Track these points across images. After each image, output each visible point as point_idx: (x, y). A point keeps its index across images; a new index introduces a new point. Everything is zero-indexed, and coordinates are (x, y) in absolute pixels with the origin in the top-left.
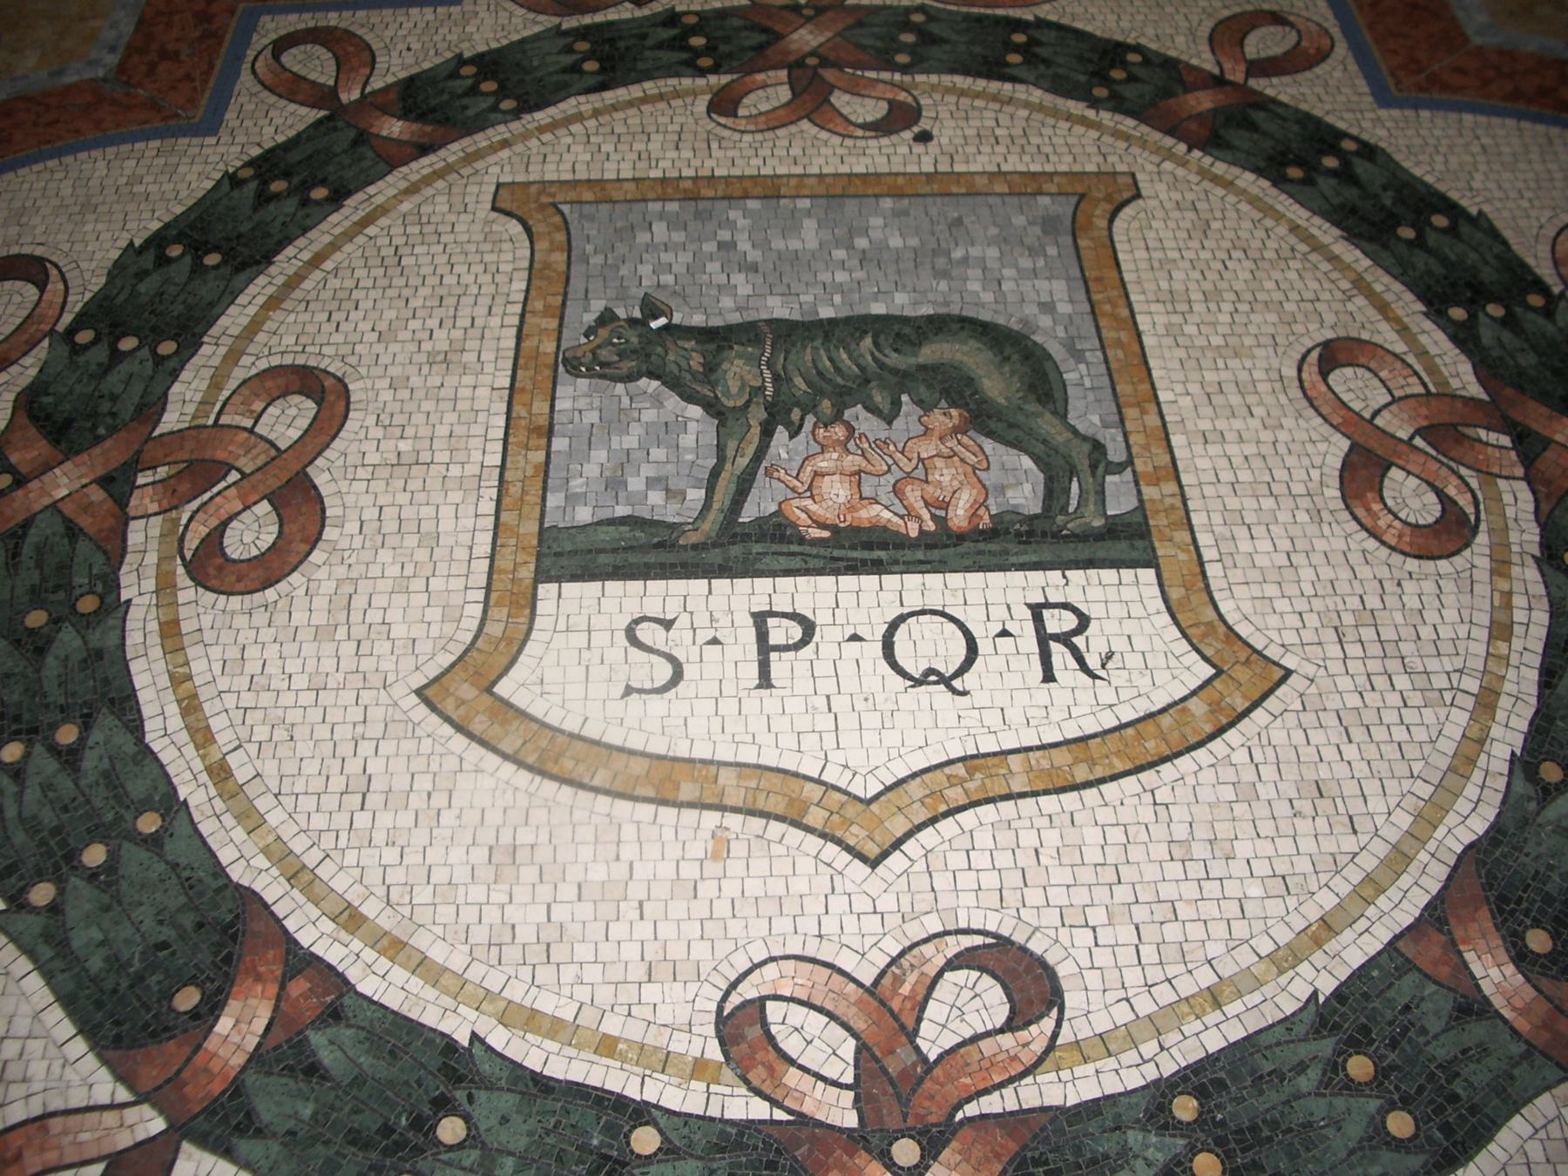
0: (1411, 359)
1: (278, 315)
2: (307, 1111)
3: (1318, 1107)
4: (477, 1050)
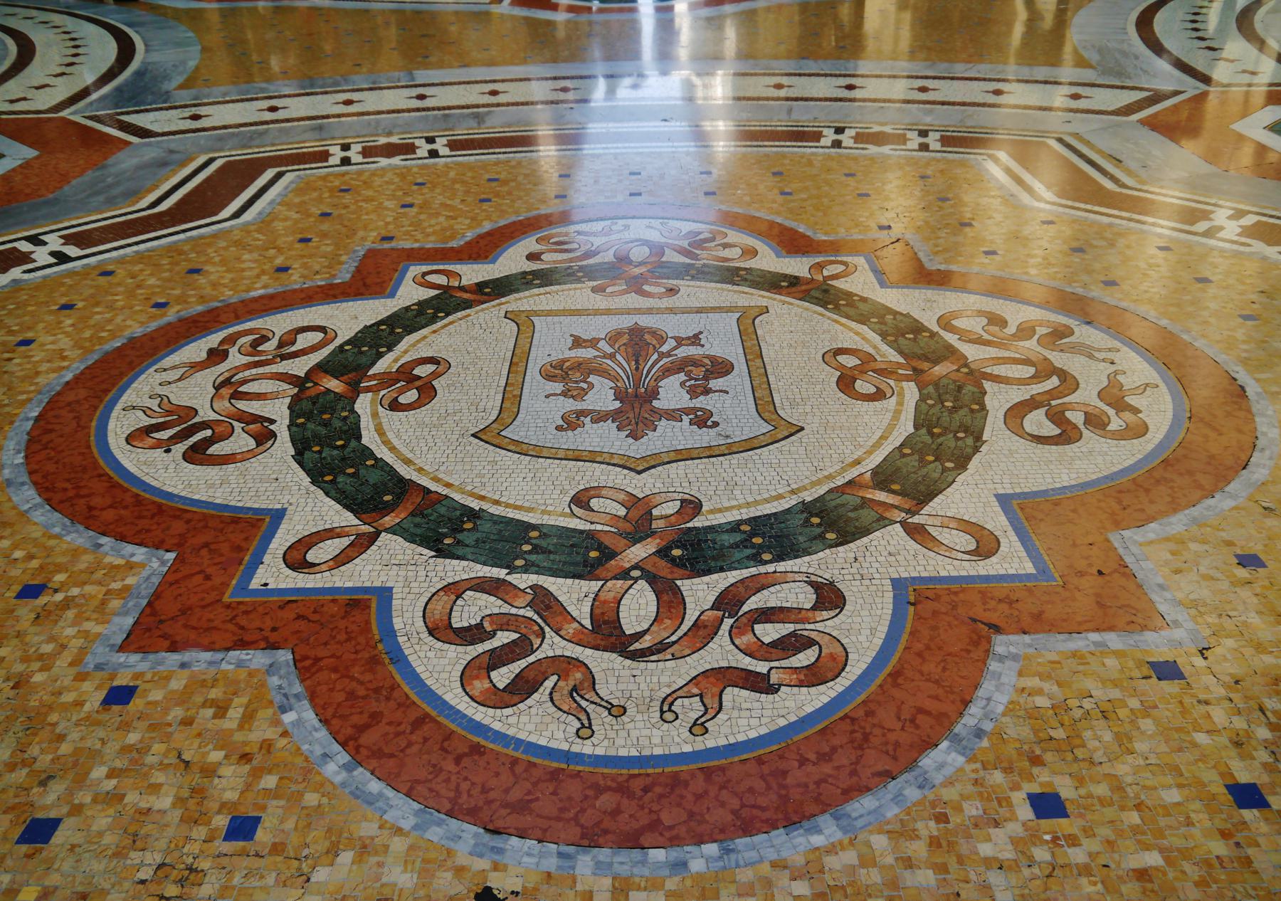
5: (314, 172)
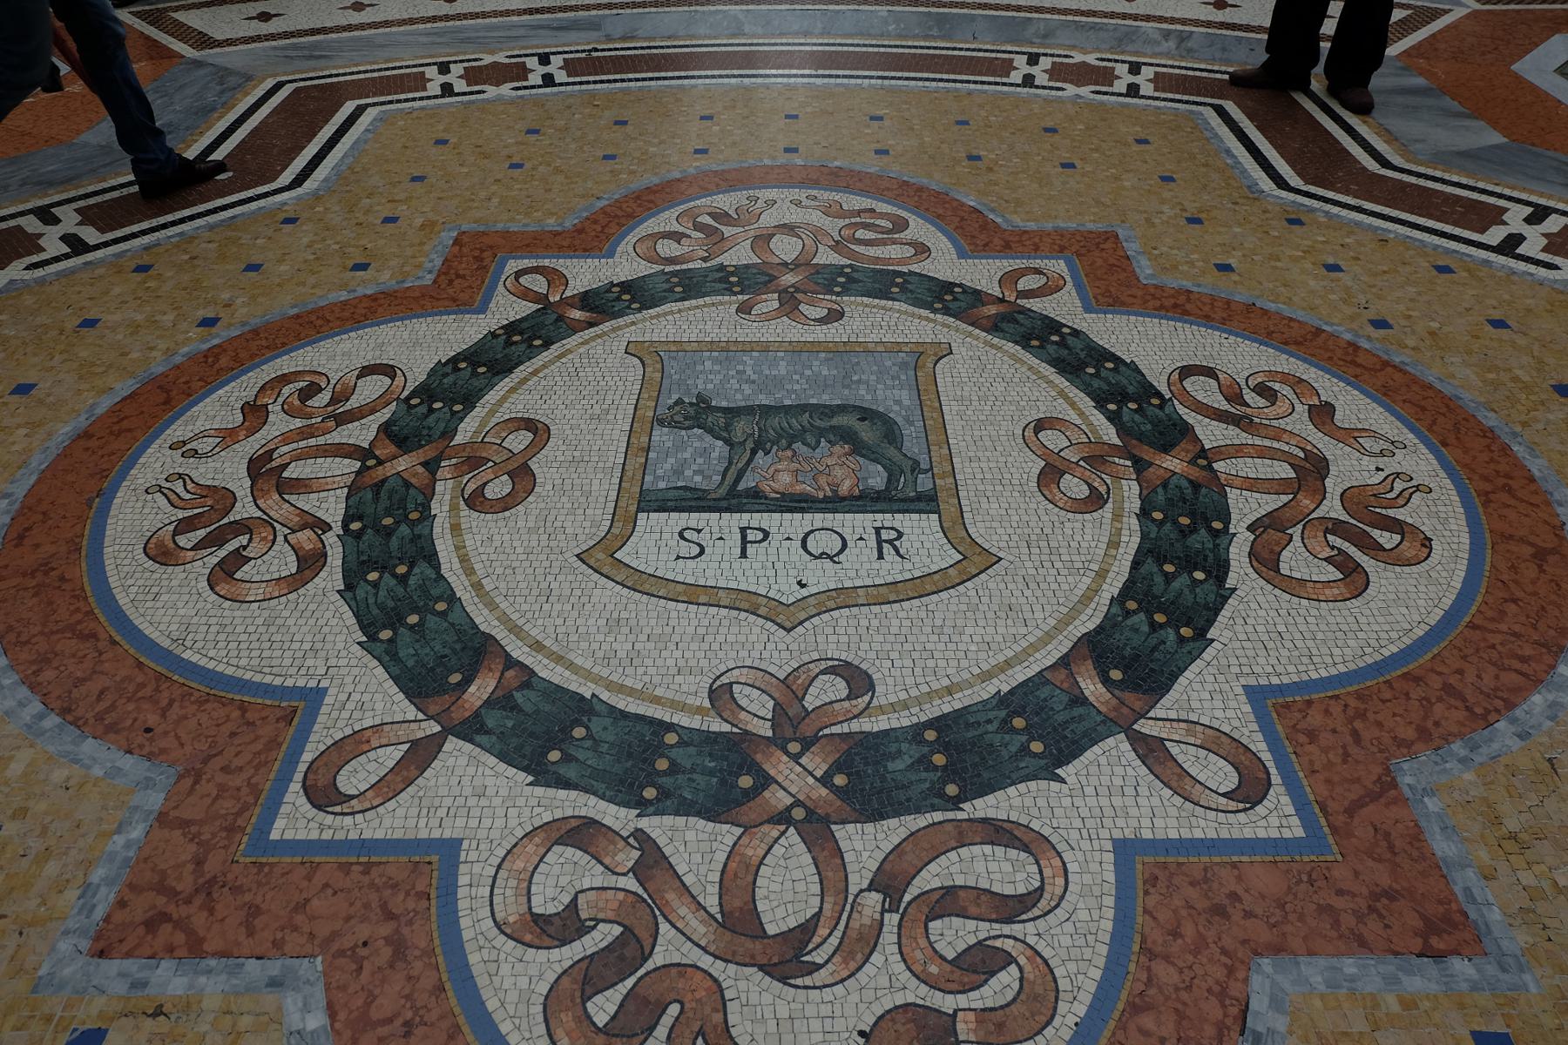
0: (1083, 427)
1: (515, 396)
2: (510, 724)
3: (997, 740)
4: (595, 700)
5: (406, 104)
